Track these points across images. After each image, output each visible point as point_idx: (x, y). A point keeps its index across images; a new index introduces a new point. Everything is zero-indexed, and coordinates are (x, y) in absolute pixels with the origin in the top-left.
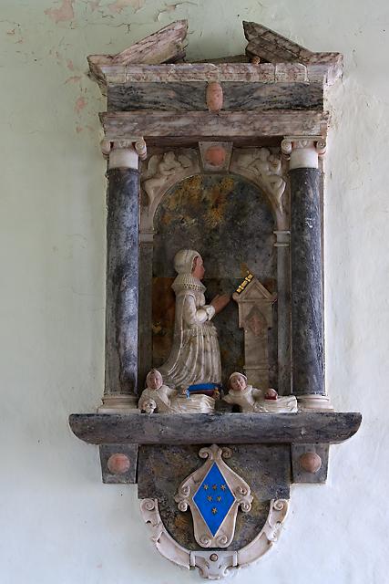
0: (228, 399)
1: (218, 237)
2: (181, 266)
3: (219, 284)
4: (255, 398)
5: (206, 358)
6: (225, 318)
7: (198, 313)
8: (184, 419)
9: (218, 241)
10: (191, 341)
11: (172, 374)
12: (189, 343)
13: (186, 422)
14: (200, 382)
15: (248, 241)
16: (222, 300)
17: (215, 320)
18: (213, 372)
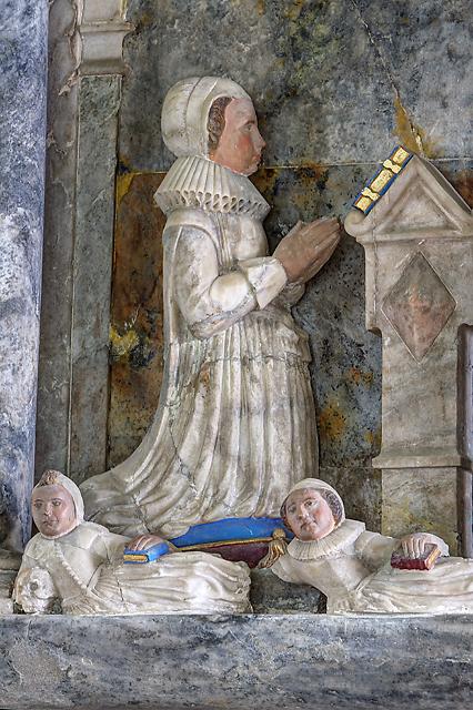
0: (283, 568)
1: (324, 30)
2: (175, 133)
3: (321, 186)
4: (367, 566)
5: (247, 431)
6: (324, 291)
7: (222, 280)
8: (131, 633)
9: (326, 41)
10: (200, 378)
11: (137, 489)
12: (195, 385)
13: (136, 643)
14: (220, 512)
15: (423, 35)
16: (308, 241)
17: (288, 306)
18: (268, 477)
